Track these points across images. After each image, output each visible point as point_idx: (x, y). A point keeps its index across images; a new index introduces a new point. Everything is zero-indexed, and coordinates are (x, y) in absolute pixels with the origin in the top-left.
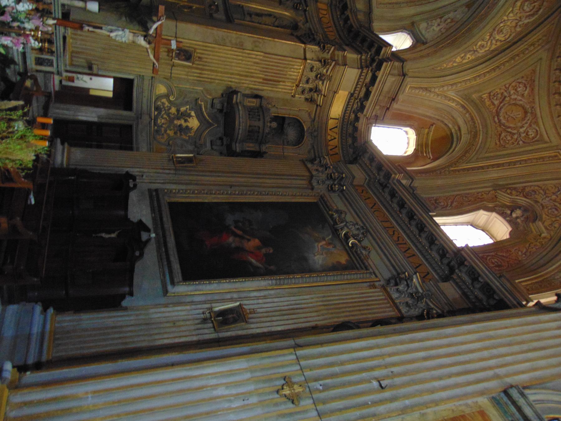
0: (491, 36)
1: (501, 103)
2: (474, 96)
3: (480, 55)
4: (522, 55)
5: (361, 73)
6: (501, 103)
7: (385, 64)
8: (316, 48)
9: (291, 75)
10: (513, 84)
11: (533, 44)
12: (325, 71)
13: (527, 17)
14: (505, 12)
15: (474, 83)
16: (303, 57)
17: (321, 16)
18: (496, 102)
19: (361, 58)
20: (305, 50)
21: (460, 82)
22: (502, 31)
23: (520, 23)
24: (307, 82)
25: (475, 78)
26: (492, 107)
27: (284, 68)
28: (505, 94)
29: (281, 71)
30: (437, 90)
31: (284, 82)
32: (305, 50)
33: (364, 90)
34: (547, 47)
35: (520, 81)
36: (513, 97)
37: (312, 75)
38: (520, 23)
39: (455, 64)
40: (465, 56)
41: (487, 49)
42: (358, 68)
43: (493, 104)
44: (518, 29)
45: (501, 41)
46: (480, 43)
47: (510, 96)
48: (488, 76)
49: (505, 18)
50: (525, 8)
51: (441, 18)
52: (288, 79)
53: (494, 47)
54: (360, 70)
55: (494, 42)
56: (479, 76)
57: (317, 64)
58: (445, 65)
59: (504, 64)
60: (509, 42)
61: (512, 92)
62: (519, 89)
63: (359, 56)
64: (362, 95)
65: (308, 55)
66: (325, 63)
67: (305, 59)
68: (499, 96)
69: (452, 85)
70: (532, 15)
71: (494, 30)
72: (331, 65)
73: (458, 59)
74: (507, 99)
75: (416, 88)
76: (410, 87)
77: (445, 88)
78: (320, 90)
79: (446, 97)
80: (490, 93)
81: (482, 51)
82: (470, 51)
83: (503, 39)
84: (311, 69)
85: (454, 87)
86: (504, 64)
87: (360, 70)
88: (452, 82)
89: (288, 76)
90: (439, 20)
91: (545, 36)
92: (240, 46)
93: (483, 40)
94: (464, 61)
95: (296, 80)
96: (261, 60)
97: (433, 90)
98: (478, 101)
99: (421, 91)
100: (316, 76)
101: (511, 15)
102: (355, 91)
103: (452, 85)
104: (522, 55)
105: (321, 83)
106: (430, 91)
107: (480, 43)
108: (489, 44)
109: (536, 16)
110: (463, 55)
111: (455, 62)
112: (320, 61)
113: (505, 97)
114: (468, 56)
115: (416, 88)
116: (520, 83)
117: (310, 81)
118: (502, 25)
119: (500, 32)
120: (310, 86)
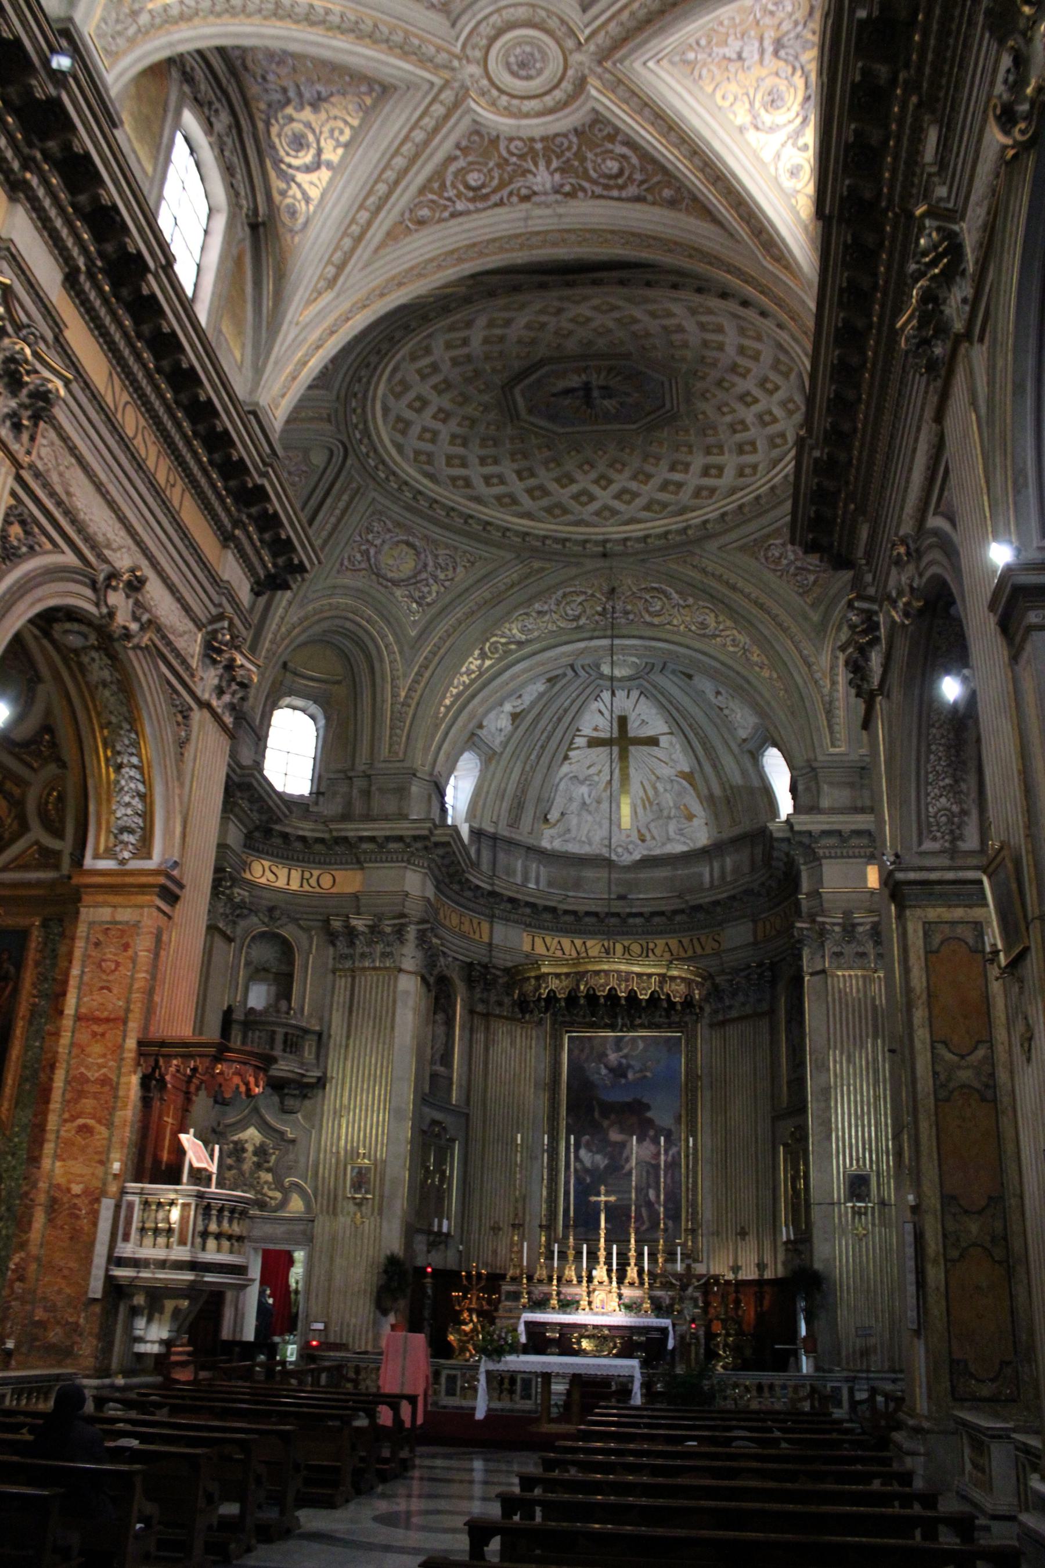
0: (715, 636)
1: (809, 571)
2: (815, 617)
3: (748, 640)
4: (725, 577)
5: (826, 858)
6: (809, 571)
7: (797, 828)
8: (806, 953)
9: (858, 990)
10: (772, 566)
11: (704, 571)
12: (837, 929)
13: (669, 598)
14: (674, 633)
15: (794, 629)
16: (822, 976)
17: (774, 933)
18: (812, 578)
19: (805, 864)
20: (812, 974)
21: (800, 652)
22: (702, 623)
23: (681, 602)
24: (863, 955)
25: (785, 630)
26: (820, 582)
27: (847, 1005)
28: (792, 570)
29: (854, 1011)
30: (826, 691)
31: (873, 999)
32: (812, 974)
33: (854, 841)
34: (698, 551)
35: (763, 560)
36: (792, 557)
37: (849, 950)
38: (681, 602)
39: (775, 676)
40: (756, 664)
41: (735, 632)
42: (821, 865)
43: (815, 582)
44: (691, 601)
45: (717, 616)
46: (731, 649)
47: (791, 563)
48: (776, 610)
49: (682, 628)
50: (658, 608)
51: (721, 709)
52: (865, 992)
53: (729, 623)
54: (824, 861)
55: (721, 627)
56: (780, 625)
57: (830, 947)
58: (782, 693)
59: (747, 596)
60: (713, 604)
61: (785, 562)
62: (777, 554)
63: (803, 867)
64: (865, 841)
65: (819, 968)
66: (822, 933)
67: (823, 971)
68: (799, 578)
69: (809, 666)
70: (664, 592)
71: (704, 635)
72: (824, 923)
73: (766, 673)
74: (799, 564)
75: (832, 732)
76: (833, 745)
77: (818, 675)
78: (872, 928)
79: (832, 668)
80: (801, 595)
81: (743, 639)
82: (748, 659)
83: (712, 615)
84: (838, 955)
85: (812, 659)
86: (747, 596)
87: (824, 861)
88: (804, 670)
89: (861, 995)
90: (726, 712)
91: (685, 562)
92: (826, 1093)
93: (725, 645)
94: (766, 662)
95: (864, 977)
96: (842, 1054)
97: (827, 698)
98: (822, 608)
99: (834, 720)
100: (849, 942)
101: (675, 622)
102: (860, 857)
103: (809, 666)
104: (725, 577)
105: (861, 929)
106: (831, 702)
107: (731, 649)
108: (728, 633)
109: (664, 587)
110: (757, 669)
111: (771, 678)
112: (822, 945)
113: (797, 568)
114: (755, 658)
115: (832, 732)
116: (767, 559)
117: (861, 950)
118: (693, 628)
119: (703, 625)
120: (869, 948)
